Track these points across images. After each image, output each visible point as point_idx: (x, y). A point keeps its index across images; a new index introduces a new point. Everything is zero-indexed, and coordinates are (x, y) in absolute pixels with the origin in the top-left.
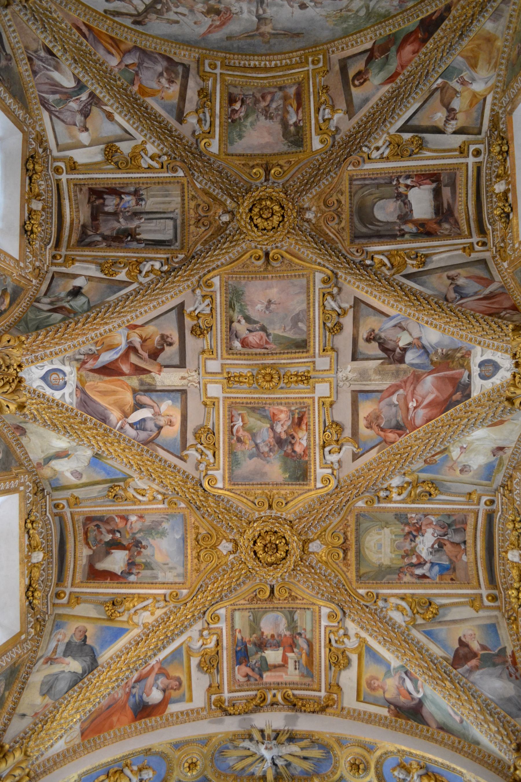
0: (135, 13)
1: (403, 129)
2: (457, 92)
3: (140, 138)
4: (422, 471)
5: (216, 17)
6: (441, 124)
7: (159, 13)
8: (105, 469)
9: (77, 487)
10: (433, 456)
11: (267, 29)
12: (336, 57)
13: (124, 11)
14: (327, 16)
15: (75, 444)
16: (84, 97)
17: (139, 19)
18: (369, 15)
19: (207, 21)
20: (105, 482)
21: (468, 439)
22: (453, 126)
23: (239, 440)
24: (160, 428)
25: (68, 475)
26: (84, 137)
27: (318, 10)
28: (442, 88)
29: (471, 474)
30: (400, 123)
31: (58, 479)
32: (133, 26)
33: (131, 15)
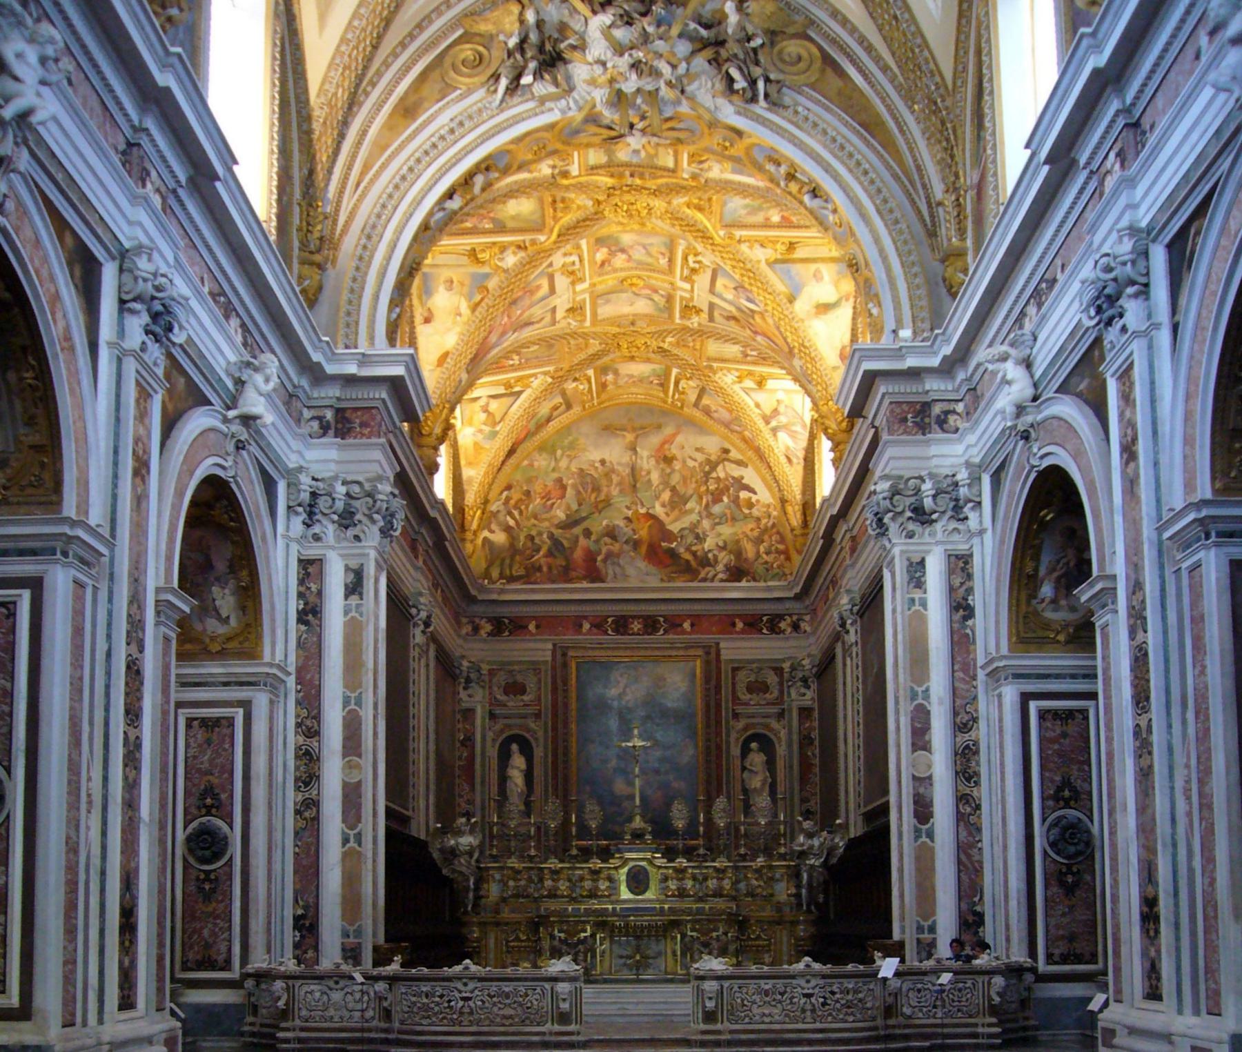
0: (726, 463)
1: (519, 393)
2: (485, 424)
3: (737, 387)
4: (487, 276)
5: (667, 453)
6: (492, 401)
7: (708, 461)
8: (790, 278)
9: (823, 260)
10: (482, 299)
11: (630, 437)
12: (576, 410)
13: (733, 466)
14: (585, 450)
15: (806, 323)
16: (774, 423)
17: (724, 456)
18: (553, 453)
19: (674, 450)
20: (794, 261)
21: (458, 329)
22: (482, 402)
23: (663, 254)
24: (735, 289)
25: (827, 278)
26: (780, 395)
27: (592, 458)
28: (495, 424)
29: (442, 279)
30: (523, 396)
31: (839, 273)
32: (731, 448)
33: (728, 460)
